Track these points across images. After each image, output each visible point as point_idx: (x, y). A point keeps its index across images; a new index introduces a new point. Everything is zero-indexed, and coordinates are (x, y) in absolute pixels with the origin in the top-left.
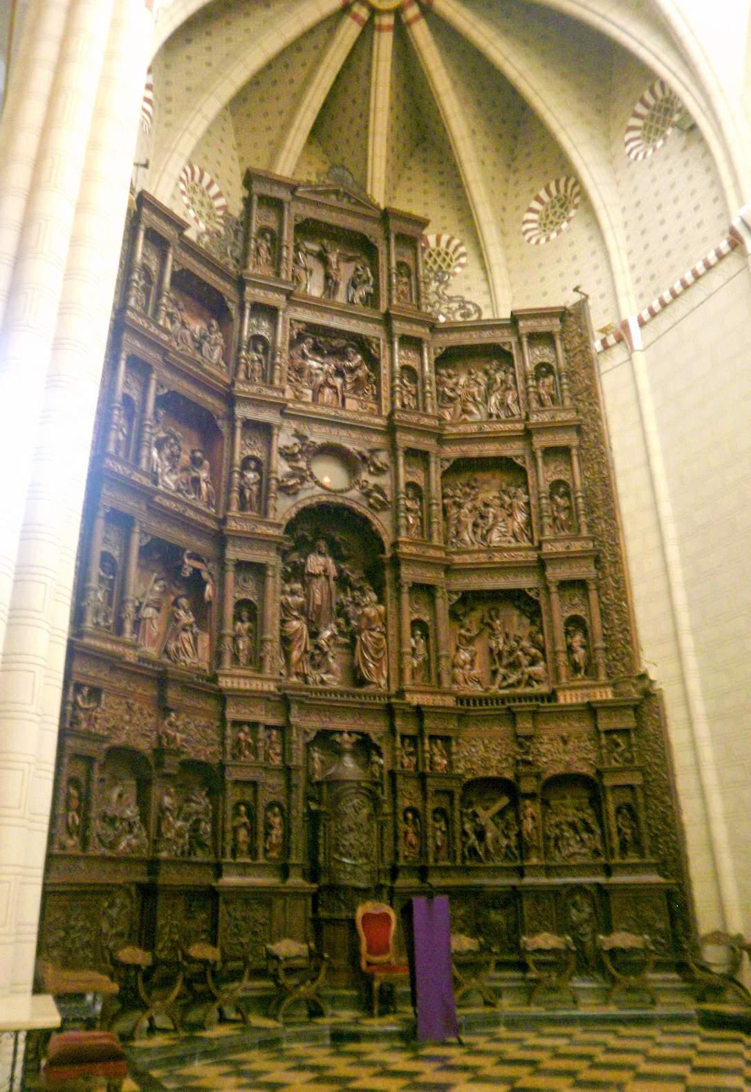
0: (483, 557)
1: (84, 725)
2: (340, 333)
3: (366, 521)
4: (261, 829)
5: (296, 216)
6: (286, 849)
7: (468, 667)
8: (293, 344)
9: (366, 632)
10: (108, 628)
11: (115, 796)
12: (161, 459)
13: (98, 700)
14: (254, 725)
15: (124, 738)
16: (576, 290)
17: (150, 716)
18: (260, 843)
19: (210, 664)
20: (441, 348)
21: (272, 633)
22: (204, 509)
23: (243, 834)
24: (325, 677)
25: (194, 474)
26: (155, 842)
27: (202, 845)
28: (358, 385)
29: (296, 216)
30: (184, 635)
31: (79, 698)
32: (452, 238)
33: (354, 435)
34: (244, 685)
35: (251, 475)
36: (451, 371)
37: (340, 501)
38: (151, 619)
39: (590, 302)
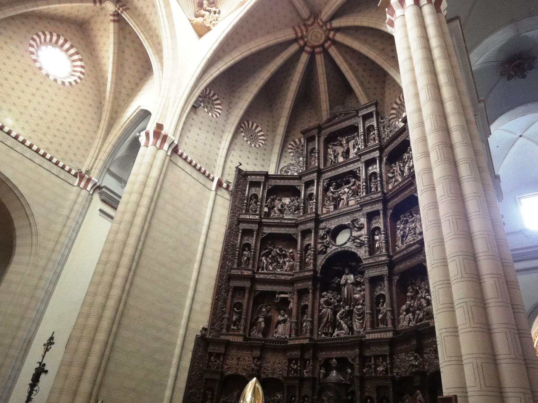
7: (405, 313)
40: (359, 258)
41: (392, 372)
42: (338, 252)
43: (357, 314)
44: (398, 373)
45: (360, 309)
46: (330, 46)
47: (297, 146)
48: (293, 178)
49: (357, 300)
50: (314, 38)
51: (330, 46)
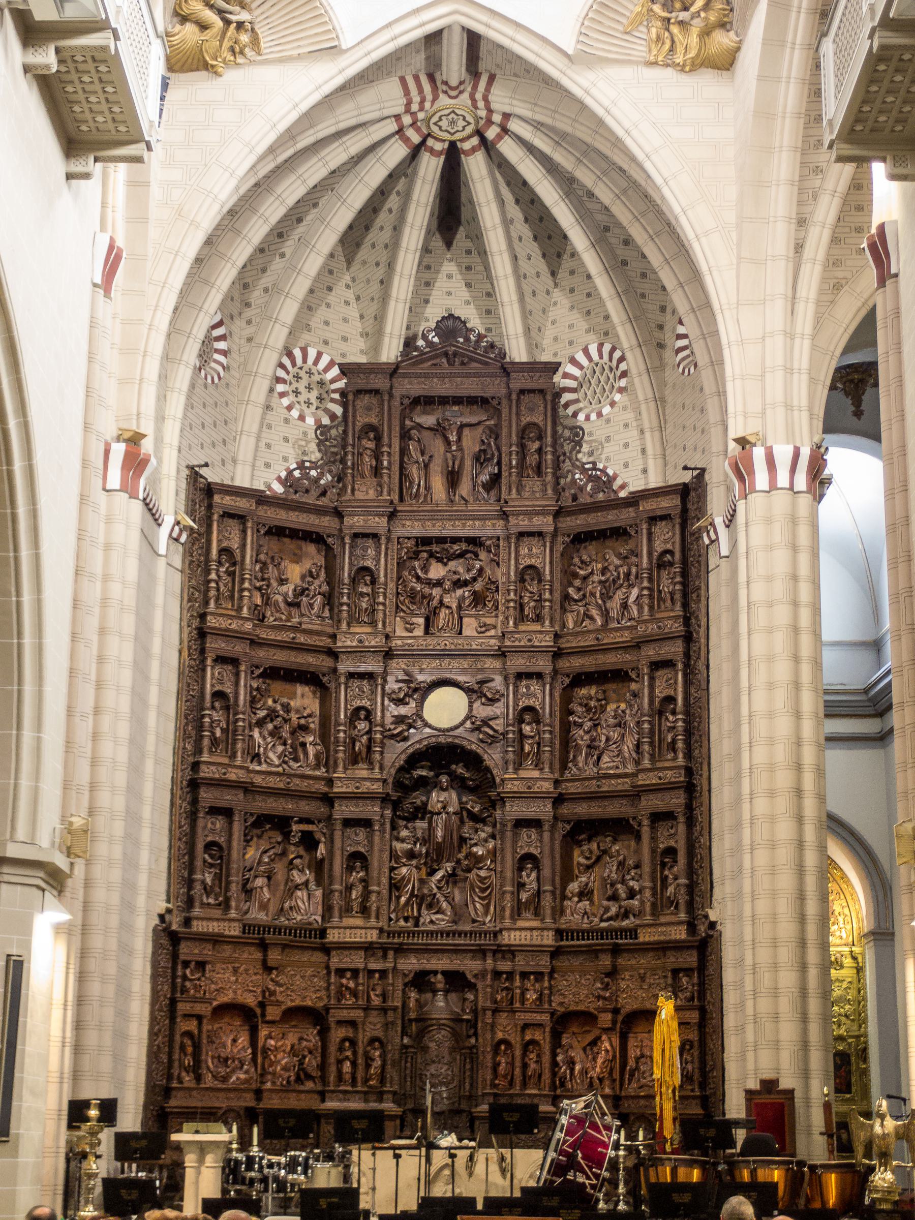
0: (592, 786)
1: (192, 992)
4: (360, 1061)
6: (382, 1080)
7: (576, 899)
9: (475, 870)
10: (219, 905)
11: (229, 1042)
12: (264, 738)
13: (204, 971)
14: (355, 972)
15: (231, 995)
16: (686, 468)
17: (256, 974)
18: (360, 1075)
19: (323, 917)
20: (569, 536)
21: (380, 886)
22: (310, 773)
23: (347, 1067)
24: (434, 917)
25: (301, 739)
26: (262, 1075)
27: (309, 1077)
28: (478, 600)
29: (403, 397)
30: (299, 893)
31: (188, 972)
33: (465, 664)
34: (349, 937)
35: (362, 726)
36: (585, 557)
37: (450, 740)
38: (261, 888)
39: (707, 477)
41: (550, 1002)
42: (438, 743)
43: (479, 888)
44: (561, 1004)
45: (485, 878)
46: (474, 150)
47: (296, 370)
49: (477, 861)
50: (444, 123)
51: (474, 150)
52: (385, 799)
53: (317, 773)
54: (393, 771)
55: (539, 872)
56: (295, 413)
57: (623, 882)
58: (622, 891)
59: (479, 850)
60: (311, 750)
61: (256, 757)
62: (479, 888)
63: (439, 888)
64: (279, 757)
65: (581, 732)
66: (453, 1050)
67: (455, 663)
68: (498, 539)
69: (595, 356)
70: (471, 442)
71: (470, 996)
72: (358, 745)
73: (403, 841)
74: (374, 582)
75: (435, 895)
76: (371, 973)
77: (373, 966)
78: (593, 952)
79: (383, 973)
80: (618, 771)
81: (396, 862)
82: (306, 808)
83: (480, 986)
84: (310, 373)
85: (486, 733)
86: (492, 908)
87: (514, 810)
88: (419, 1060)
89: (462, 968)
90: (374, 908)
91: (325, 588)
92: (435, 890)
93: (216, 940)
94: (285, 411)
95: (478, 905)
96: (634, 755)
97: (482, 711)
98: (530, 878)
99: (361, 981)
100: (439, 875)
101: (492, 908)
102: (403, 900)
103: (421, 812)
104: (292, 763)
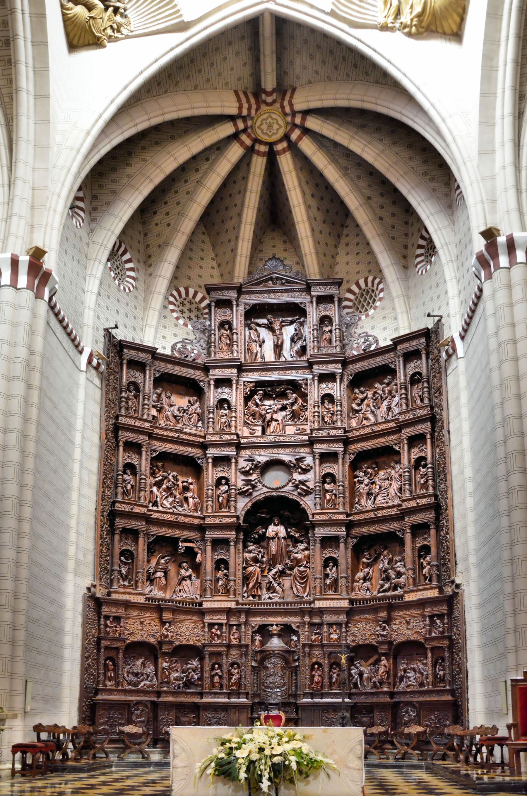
2: (280, 383)
3: (298, 504)
5: (245, 305)
7: (362, 581)
8: (247, 398)
17: (155, 626)
22: (191, 514)
28: (295, 416)
29: (245, 305)
32: (375, 278)
33: (288, 450)
37: (279, 494)
38: (160, 578)
40: (304, 511)
43: (300, 577)
44: (353, 641)
45: (303, 572)
47: (182, 300)
48: (193, 366)
49: (298, 562)
52: (237, 528)
53: (195, 514)
54: (243, 513)
55: (337, 568)
56: (181, 321)
57: (392, 568)
58: (392, 574)
59: (299, 556)
60: (191, 500)
61: (155, 504)
62: (300, 577)
63: (274, 579)
64: (170, 504)
65: (363, 485)
66: (283, 668)
67: (282, 450)
68: (307, 380)
69: (363, 286)
70: (289, 331)
71: (295, 638)
72: (221, 499)
73: (250, 552)
74: (229, 408)
75: (271, 582)
76: (231, 626)
77: (233, 621)
78: (375, 610)
79: (239, 625)
80: (387, 505)
81: (246, 564)
82: (188, 534)
83: (300, 631)
84: (190, 303)
85: (301, 489)
86: (308, 589)
87: (320, 532)
88: (262, 675)
89: (289, 622)
90: (232, 589)
91: (199, 410)
92: (272, 580)
93: (128, 605)
94: (175, 320)
95: (298, 587)
96: (399, 494)
97: (298, 477)
98: (332, 572)
99: (224, 630)
100: (275, 570)
101: (308, 589)
102: (251, 585)
103: (262, 540)
104: (178, 508)
